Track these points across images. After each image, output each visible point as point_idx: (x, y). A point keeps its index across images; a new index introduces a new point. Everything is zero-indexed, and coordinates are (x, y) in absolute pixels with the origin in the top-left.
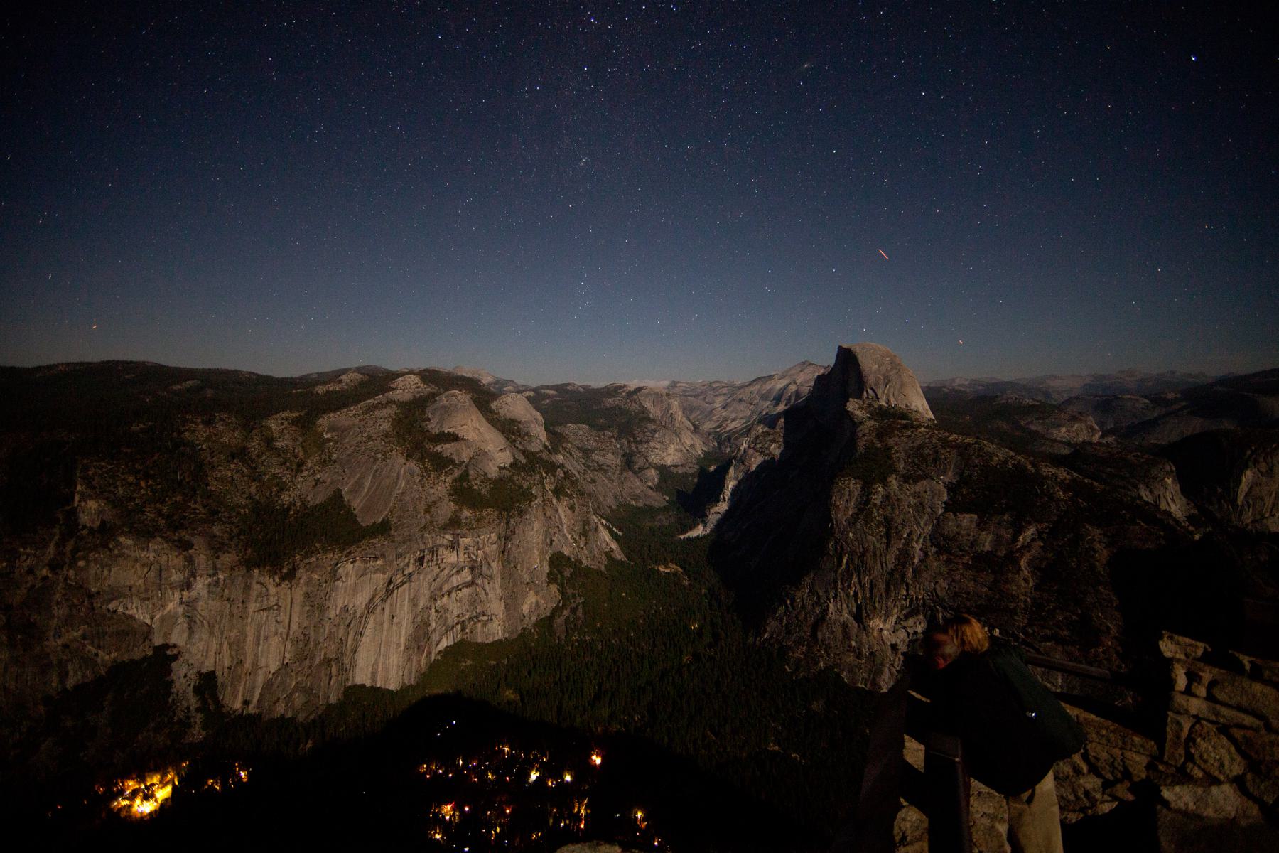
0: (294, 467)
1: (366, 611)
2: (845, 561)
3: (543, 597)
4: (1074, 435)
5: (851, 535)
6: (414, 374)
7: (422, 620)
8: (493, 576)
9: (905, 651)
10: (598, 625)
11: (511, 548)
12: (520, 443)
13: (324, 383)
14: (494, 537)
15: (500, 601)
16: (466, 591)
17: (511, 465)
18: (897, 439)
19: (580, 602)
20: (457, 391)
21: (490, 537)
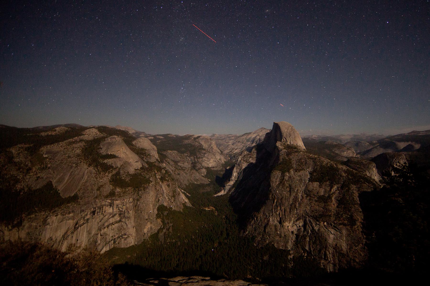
0: (25, 171)
1: (63, 239)
2: (275, 201)
3: (154, 225)
4: (348, 154)
5: (277, 191)
6: (95, 128)
7: (93, 240)
8: (130, 217)
9: (296, 233)
10: (179, 235)
11: (139, 204)
12: (146, 159)
13: (46, 131)
14: (131, 200)
15: (133, 228)
16: (116, 225)
17: (141, 168)
18: (293, 156)
19: (171, 225)
20: (116, 136)
21: (129, 200)
